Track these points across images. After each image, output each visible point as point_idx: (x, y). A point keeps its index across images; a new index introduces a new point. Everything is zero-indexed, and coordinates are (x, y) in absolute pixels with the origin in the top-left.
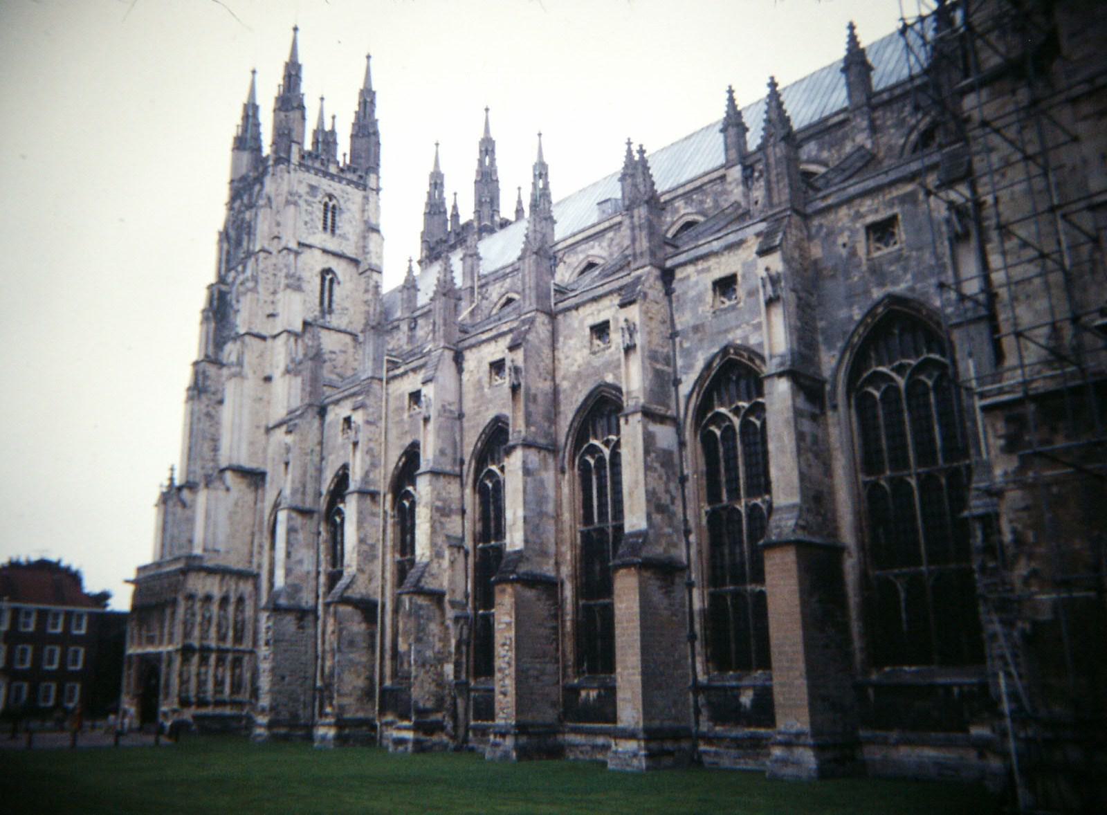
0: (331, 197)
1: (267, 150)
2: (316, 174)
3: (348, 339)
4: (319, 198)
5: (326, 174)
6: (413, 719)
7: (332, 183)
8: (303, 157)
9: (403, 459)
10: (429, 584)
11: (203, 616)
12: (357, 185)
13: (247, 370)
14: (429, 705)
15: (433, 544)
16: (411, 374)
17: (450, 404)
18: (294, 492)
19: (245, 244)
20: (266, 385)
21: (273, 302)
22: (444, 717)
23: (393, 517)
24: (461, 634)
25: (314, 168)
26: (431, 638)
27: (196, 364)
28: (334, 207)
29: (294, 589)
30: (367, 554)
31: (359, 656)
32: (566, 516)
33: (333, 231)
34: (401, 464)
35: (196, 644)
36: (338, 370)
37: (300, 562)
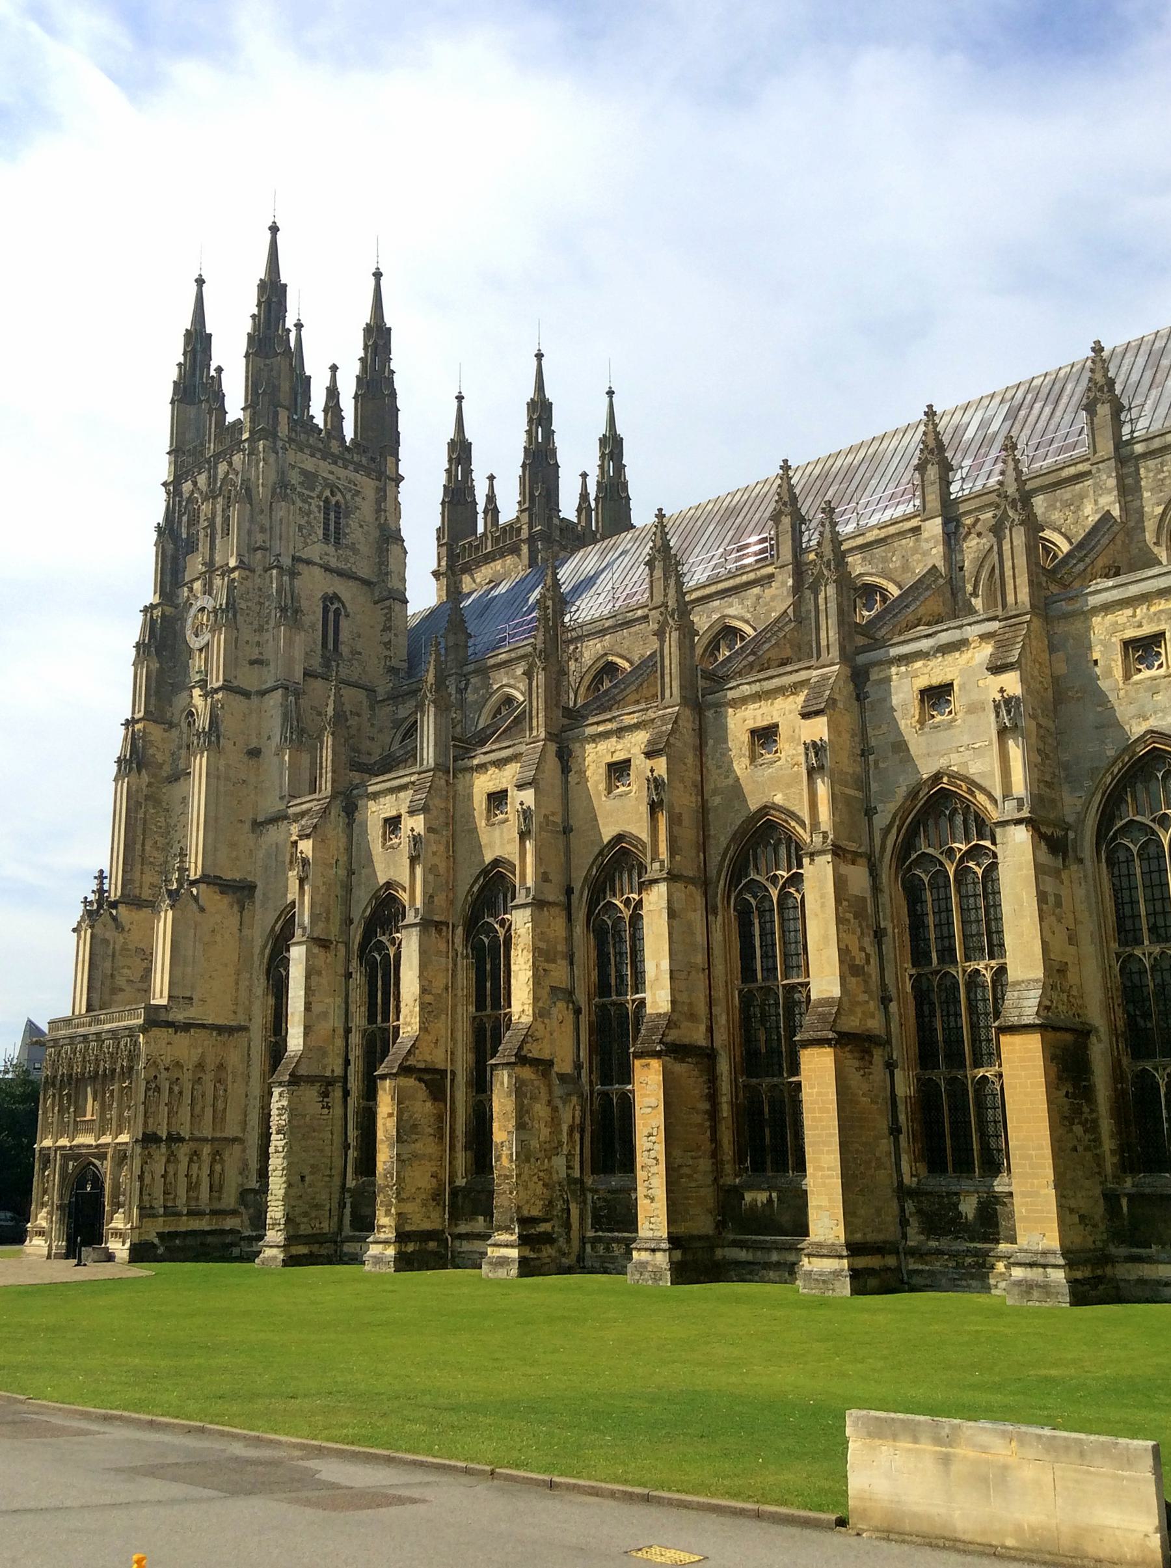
1: (235, 407)
2: (312, 456)
3: (361, 695)
7: (333, 468)
8: (291, 430)
14: (535, 1213)
16: (492, 770)
17: (553, 814)
23: (467, 956)
25: (311, 446)
27: (127, 723)
31: (426, 1146)
32: (719, 969)
34: (475, 889)
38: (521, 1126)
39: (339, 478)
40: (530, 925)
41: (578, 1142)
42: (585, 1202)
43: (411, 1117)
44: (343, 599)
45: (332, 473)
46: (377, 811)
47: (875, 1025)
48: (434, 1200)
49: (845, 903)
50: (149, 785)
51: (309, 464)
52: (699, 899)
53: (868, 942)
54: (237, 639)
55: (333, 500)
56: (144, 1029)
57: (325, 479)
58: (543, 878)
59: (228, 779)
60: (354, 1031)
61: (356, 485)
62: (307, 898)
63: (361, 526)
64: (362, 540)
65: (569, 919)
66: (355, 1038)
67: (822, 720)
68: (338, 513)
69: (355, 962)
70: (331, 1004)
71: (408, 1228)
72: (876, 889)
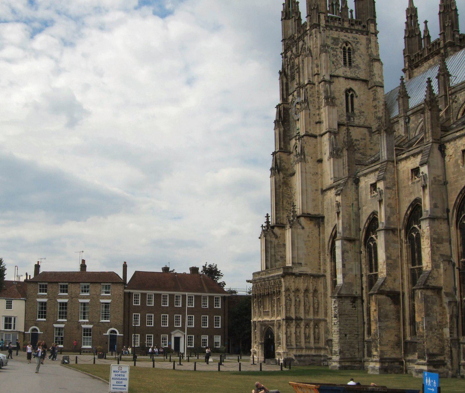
0: (347, 43)
2: (336, 30)
3: (365, 131)
4: (340, 46)
5: (343, 29)
6: (427, 359)
7: (346, 34)
8: (327, 21)
9: (411, 209)
10: (433, 283)
11: (296, 300)
12: (362, 33)
13: (308, 158)
14: (435, 351)
15: (433, 260)
16: (412, 158)
18: (344, 229)
19: (297, 78)
20: (319, 165)
21: (319, 115)
22: (445, 358)
23: (407, 243)
24: (453, 311)
25: (335, 27)
26: (435, 314)
27: (274, 154)
28: (349, 49)
29: (347, 284)
30: (391, 265)
31: (392, 324)
33: (350, 64)
35: (293, 317)
36: (361, 151)
37: (351, 269)
38: (427, 315)
39: (349, 38)
40: (428, 227)
42: (459, 348)
44: (355, 90)
45: (345, 36)
46: (366, 182)
48: (397, 346)
50: (283, 178)
51: (335, 34)
54: (309, 114)
55: (347, 48)
56: (283, 276)
57: (343, 39)
58: (434, 206)
60: (364, 275)
61: (357, 39)
62: (340, 221)
63: (361, 57)
64: (362, 62)
65: (448, 224)
66: (364, 279)
68: (349, 53)
70: (353, 265)
71: (385, 357)
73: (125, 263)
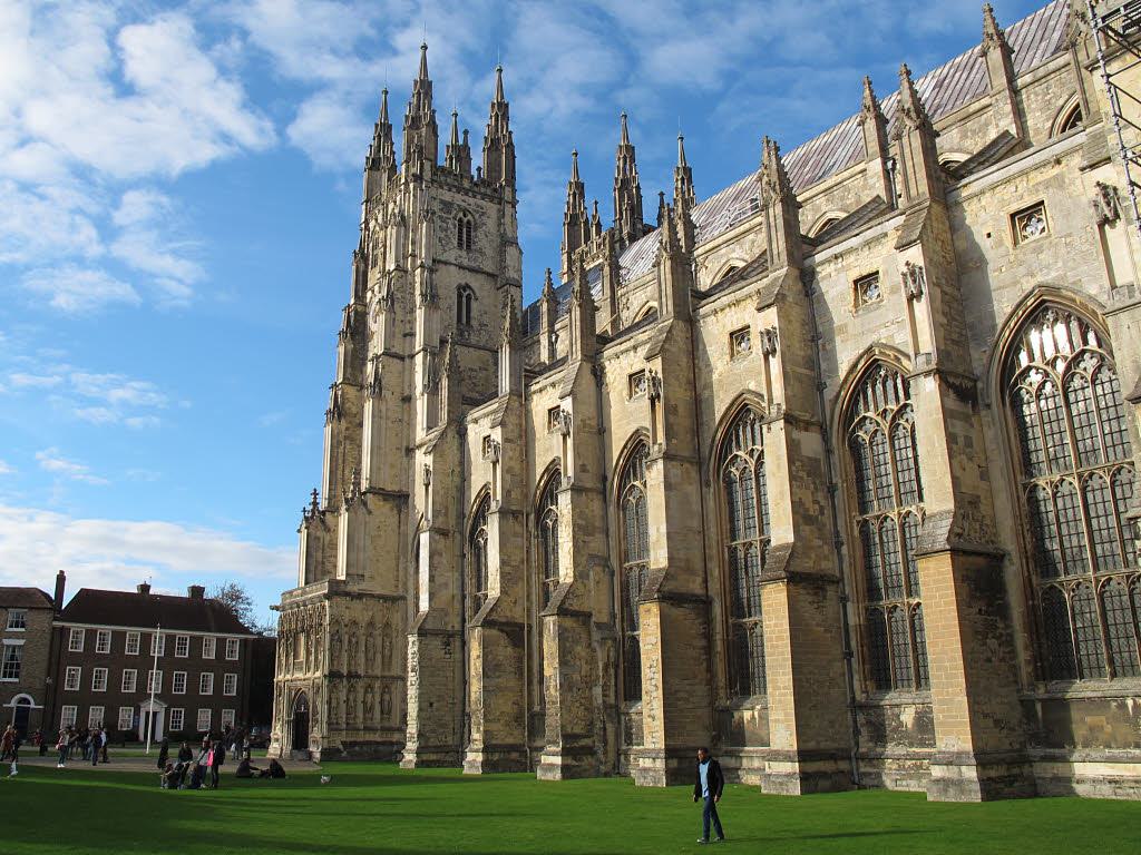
2: (450, 190)
7: (465, 198)
8: (434, 174)
10: (575, 605)
11: (350, 642)
14: (577, 730)
17: (589, 419)
19: (380, 263)
20: (406, 406)
22: (594, 742)
28: (469, 222)
31: (509, 681)
33: (468, 246)
38: (563, 663)
40: (570, 506)
41: (613, 676)
42: (619, 722)
43: (494, 659)
47: (829, 566)
49: (798, 464)
50: (347, 429)
51: (447, 196)
52: (694, 474)
53: (820, 497)
55: (465, 220)
56: (327, 597)
59: (387, 418)
64: (487, 246)
65: (605, 501)
67: (774, 310)
68: (469, 228)
69: (467, 545)
71: (494, 742)
72: (829, 452)
73: (62, 572)
